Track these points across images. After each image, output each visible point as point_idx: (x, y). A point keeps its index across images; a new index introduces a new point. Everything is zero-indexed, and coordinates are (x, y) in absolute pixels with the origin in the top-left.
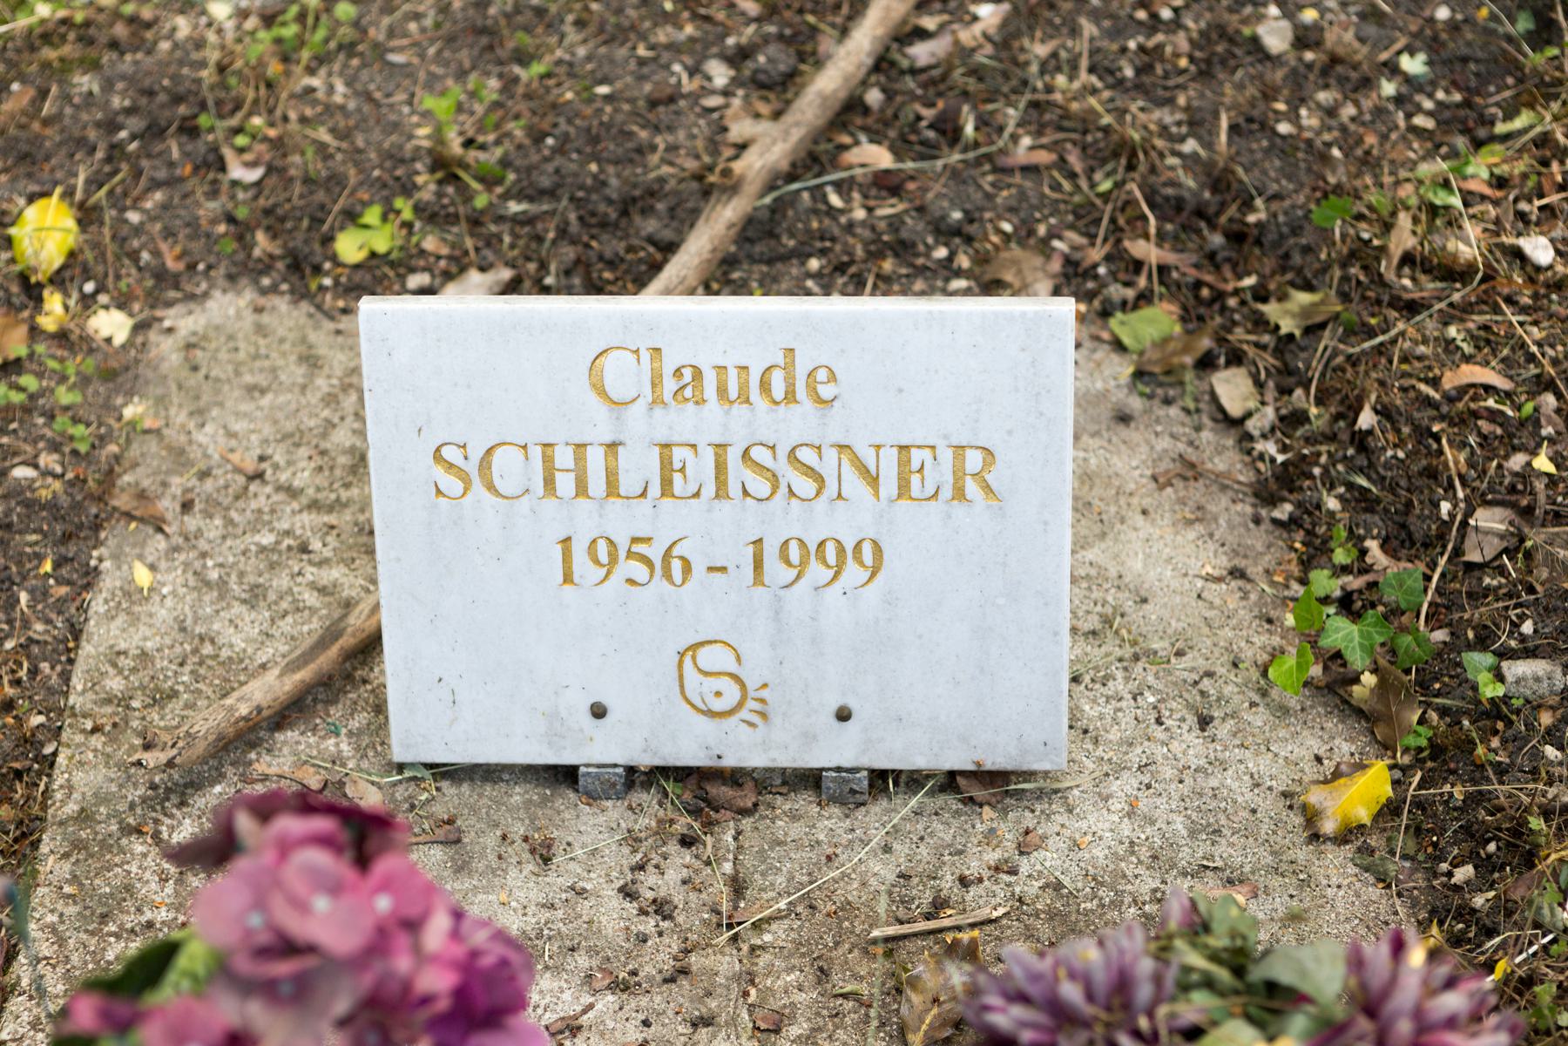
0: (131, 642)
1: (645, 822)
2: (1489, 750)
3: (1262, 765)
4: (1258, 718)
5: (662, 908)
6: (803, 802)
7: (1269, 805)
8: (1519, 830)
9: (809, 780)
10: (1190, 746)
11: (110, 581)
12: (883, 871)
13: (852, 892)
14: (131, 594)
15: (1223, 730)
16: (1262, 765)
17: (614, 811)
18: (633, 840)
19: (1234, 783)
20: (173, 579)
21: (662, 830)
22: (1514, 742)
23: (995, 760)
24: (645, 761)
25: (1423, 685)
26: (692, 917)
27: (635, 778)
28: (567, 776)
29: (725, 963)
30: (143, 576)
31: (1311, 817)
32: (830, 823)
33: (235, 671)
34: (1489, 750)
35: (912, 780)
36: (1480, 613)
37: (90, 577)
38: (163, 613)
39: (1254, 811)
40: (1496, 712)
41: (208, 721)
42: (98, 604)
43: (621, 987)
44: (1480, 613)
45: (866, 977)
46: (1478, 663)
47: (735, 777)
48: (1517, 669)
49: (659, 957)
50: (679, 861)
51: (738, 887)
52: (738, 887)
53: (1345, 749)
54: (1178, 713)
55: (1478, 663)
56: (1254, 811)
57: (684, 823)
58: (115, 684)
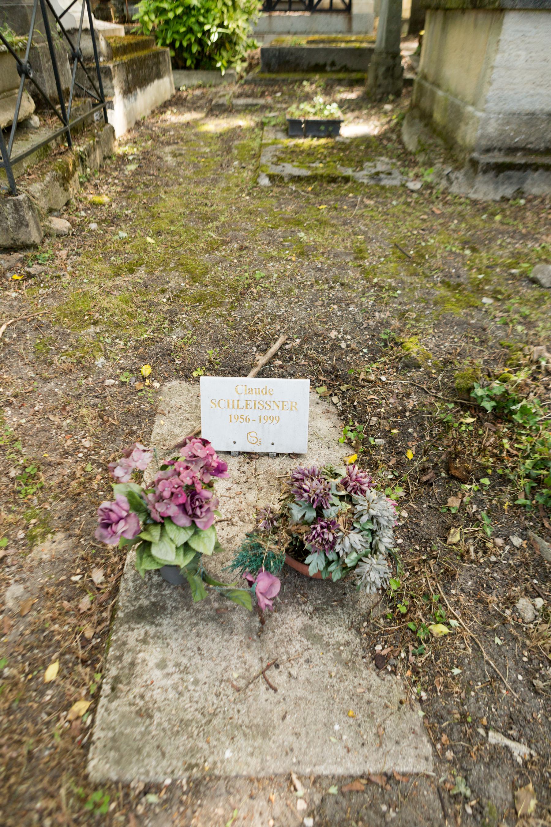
0: (161, 432)
1: (241, 460)
2: (373, 452)
3: (337, 454)
4: (337, 448)
5: (244, 472)
6: (266, 458)
7: (338, 460)
8: (377, 463)
9: (267, 454)
10: (326, 451)
11: (157, 423)
12: (278, 468)
13: (273, 471)
14: (160, 425)
15: (331, 449)
16: (337, 454)
17: (237, 458)
18: (239, 463)
19: (333, 457)
20: (167, 423)
21: (244, 461)
22: (376, 451)
23: (296, 452)
24: (242, 451)
25: (363, 443)
26: (248, 474)
27: (240, 453)
28: (229, 453)
29: (254, 480)
30: (162, 422)
31: (345, 462)
32: (270, 461)
33: (177, 436)
34: (373, 452)
35: (283, 455)
36: (372, 432)
37: (154, 422)
38: (165, 428)
39: (401, 702)
40: (374, 447)
41: (174, 443)
42: (155, 426)
43: (237, 483)
44: (372, 432)
45: (276, 483)
46: (371, 439)
47: (255, 454)
48: (377, 440)
49: (243, 479)
50: (247, 466)
51: (256, 470)
52: (256, 470)
53: (350, 452)
54: (325, 447)
55: (371, 439)
56: (401, 702)
57: (247, 460)
58: (158, 438)
